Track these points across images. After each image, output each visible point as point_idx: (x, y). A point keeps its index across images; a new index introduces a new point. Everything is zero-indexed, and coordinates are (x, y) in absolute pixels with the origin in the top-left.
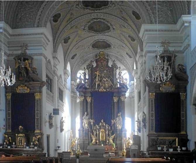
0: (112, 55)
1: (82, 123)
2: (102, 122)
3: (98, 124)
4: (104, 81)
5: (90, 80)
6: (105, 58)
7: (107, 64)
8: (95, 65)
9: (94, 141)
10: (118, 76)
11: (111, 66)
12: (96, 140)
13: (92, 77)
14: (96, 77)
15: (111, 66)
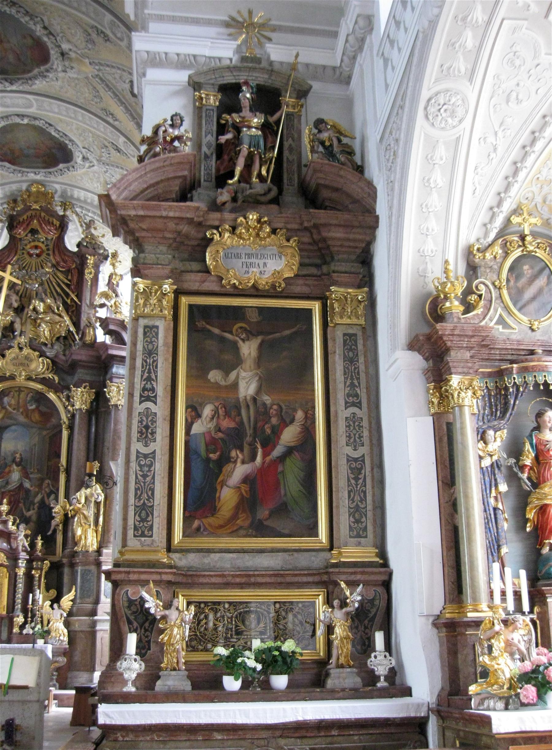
0: (85, 202)
4: (35, 309)
6: (53, 214)
7: (60, 239)
11: (75, 249)
15: (75, 249)
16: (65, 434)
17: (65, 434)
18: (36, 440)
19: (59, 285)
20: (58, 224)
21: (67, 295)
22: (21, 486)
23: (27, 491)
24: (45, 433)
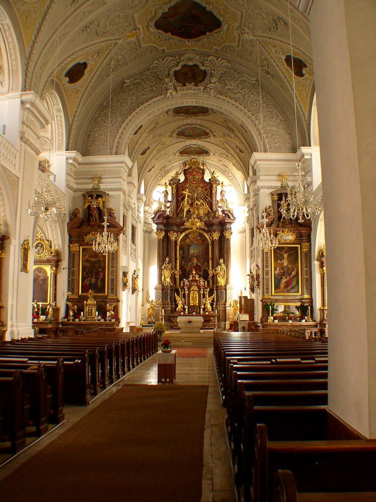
1: (160, 275)
2: (193, 274)
3: (187, 278)
4: (197, 204)
5: (175, 201)
6: (200, 169)
7: (203, 177)
8: (182, 178)
9: (180, 306)
10: (219, 197)
11: (208, 181)
12: (184, 304)
13: (178, 197)
14: (184, 198)
15: (208, 181)
16: (210, 247)
17: (210, 247)
18: (201, 249)
19: (204, 195)
20: (201, 172)
21: (207, 198)
22: (197, 264)
23: (199, 266)
24: (204, 247)
